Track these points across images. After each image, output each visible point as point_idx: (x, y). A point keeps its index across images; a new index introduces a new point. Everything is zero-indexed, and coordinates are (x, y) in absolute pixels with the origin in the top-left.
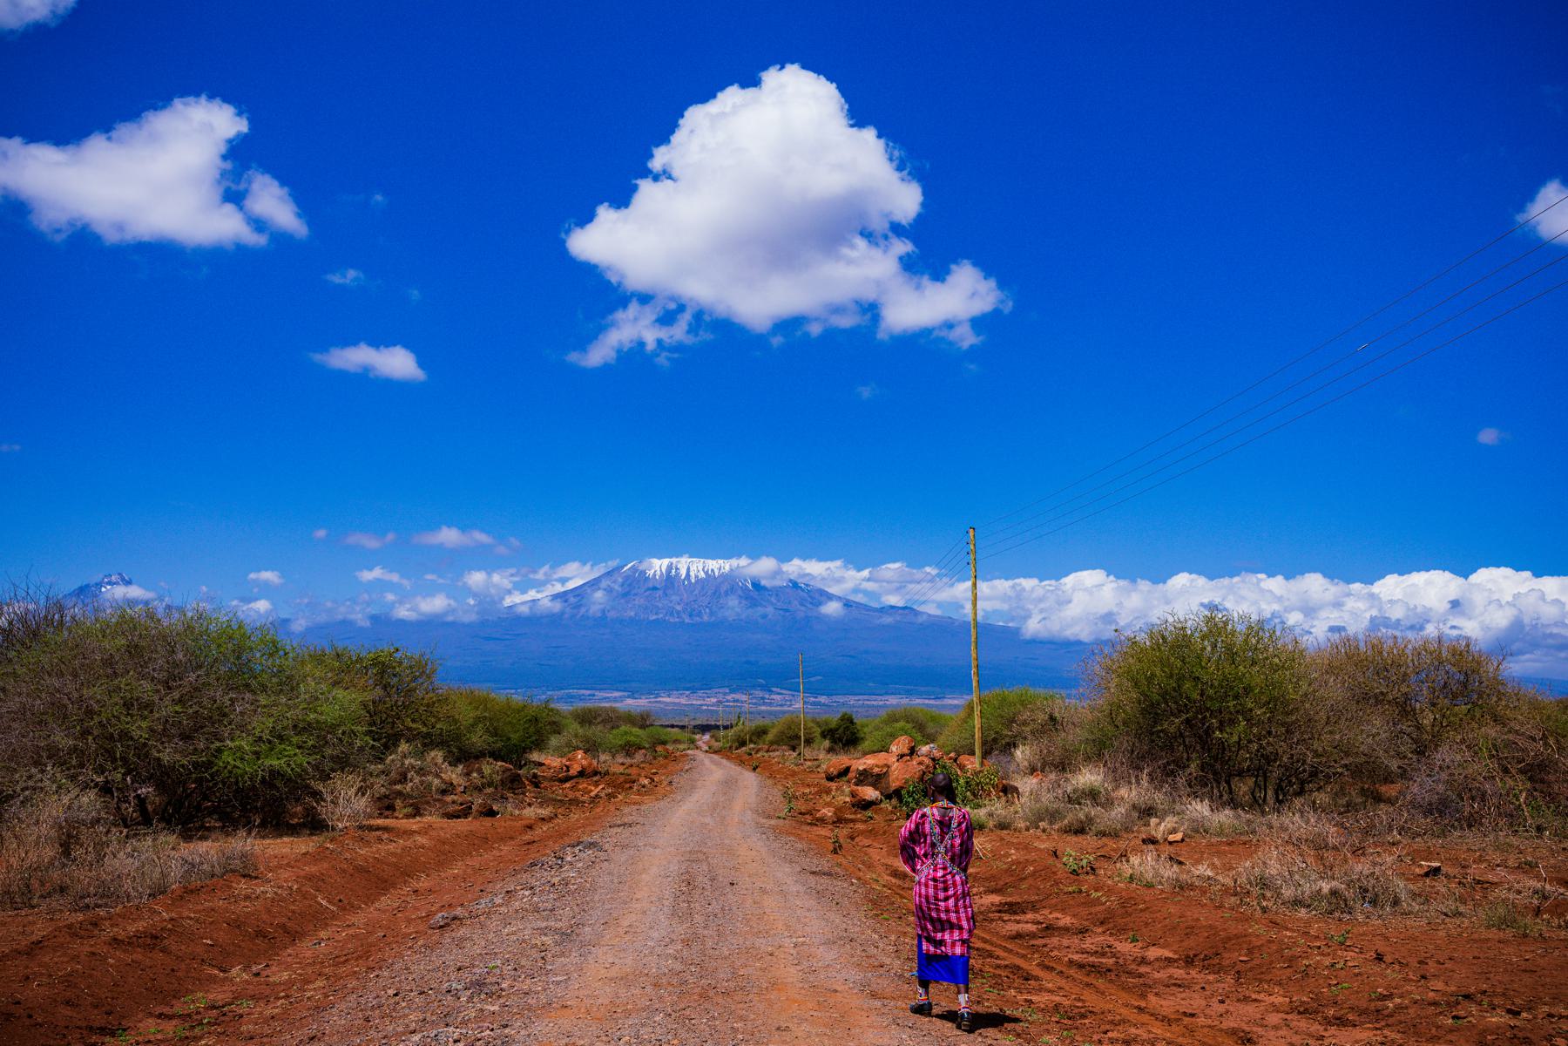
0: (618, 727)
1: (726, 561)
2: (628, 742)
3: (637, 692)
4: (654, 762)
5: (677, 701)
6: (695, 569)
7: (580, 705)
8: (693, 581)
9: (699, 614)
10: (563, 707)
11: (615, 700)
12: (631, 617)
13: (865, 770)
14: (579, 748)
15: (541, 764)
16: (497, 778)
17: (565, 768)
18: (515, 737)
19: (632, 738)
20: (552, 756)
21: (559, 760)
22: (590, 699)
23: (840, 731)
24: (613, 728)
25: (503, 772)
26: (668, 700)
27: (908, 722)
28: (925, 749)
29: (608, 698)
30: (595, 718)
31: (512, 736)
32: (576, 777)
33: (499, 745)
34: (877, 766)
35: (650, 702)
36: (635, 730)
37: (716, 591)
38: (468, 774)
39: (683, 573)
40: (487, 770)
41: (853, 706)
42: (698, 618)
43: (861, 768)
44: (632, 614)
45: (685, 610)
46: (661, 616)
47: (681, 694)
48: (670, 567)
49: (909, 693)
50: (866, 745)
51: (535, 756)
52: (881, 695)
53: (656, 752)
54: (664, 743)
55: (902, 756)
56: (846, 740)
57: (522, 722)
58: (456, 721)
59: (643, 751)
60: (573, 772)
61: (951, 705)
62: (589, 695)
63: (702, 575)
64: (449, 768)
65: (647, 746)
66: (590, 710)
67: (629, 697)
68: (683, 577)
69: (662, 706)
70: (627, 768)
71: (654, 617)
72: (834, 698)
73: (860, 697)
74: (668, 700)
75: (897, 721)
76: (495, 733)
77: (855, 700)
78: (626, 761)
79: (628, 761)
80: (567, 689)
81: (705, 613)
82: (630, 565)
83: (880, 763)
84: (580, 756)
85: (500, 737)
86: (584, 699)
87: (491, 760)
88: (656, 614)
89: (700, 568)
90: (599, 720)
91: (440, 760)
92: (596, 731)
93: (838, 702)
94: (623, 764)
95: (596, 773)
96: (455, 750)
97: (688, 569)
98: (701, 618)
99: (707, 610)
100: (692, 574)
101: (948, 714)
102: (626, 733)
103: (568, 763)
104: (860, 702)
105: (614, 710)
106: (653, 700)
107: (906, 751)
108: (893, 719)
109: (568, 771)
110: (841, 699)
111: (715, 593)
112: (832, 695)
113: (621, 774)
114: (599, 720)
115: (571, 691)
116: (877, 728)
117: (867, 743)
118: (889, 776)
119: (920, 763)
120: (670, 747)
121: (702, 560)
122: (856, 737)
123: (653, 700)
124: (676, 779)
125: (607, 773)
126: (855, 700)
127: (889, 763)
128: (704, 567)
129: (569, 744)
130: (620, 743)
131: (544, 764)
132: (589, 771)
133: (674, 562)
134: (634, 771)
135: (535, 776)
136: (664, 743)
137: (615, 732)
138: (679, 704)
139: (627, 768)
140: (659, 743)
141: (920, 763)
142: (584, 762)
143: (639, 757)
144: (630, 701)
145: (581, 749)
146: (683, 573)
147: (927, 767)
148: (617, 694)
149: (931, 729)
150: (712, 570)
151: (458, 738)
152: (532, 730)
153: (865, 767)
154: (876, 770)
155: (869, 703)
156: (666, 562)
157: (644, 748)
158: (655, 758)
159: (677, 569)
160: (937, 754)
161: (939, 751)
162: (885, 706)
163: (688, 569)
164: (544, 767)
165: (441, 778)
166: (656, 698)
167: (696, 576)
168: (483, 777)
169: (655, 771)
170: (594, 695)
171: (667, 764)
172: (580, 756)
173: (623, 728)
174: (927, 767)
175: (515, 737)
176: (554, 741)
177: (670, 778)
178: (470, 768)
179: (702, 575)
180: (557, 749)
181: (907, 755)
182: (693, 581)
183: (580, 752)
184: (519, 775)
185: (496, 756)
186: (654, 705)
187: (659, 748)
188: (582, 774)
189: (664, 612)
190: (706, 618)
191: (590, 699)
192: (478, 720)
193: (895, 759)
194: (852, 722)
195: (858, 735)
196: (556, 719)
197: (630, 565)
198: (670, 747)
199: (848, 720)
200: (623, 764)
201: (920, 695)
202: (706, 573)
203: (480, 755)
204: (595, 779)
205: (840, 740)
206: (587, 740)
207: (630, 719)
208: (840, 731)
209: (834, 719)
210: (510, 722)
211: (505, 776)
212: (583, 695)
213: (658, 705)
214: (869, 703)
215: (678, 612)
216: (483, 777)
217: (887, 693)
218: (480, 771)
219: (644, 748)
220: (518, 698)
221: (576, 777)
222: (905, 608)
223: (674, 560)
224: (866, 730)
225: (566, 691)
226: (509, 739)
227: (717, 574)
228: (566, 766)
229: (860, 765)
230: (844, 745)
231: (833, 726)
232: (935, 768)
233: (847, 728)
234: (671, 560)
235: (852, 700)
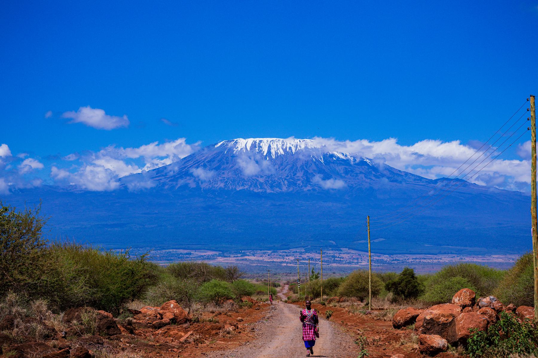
0: (209, 280)
1: (301, 140)
2: (218, 293)
3: (227, 251)
4: (240, 310)
5: (261, 259)
6: (275, 147)
7: (176, 262)
8: (274, 157)
9: (279, 186)
10: (162, 264)
11: (209, 258)
12: (220, 188)
13: (431, 319)
14: (172, 298)
15: (137, 312)
16: (94, 325)
17: (159, 316)
18: (113, 288)
19: (221, 290)
20: (149, 305)
21: (153, 309)
22: (187, 257)
23: (403, 284)
24: (205, 281)
25: (100, 319)
26: (252, 258)
27: (463, 277)
28: (485, 300)
29: (202, 256)
30: (189, 273)
31: (111, 287)
32: (169, 324)
33: (99, 295)
34: (443, 316)
35: (238, 260)
36: (223, 283)
37: (293, 165)
38: (68, 321)
39: (265, 150)
40: (85, 317)
41: (412, 264)
42: (278, 189)
43: (428, 317)
44: (222, 185)
45: (266, 182)
46: (246, 187)
47: (264, 253)
48: (254, 145)
49: (459, 253)
50: (427, 296)
51: (134, 305)
52: (436, 254)
53: (242, 301)
54: (249, 294)
55: (464, 307)
56: (408, 292)
57: (119, 275)
58: (58, 274)
59: (231, 301)
60: (166, 320)
61: (496, 263)
62: (187, 254)
63: (281, 152)
64: (52, 315)
65: (234, 297)
66: (185, 266)
67: (219, 256)
68: (265, 154)
69: (248, 263)
70: (216, 316)
71: (241, 188)
72: (395, 257)
73: (418, 256)
74: (252, 258)
75: (454, 276)
76: (96, 285)
77: (413, 259)
78: (215, 309)
79: (217, 309)
80: (168, 249)
81: (284, 184)
82: (219, 144)
83: (447, 313)
84: (172, 305)
85: (100, 288)
86: (181, 257)
87: (89, 309)
88: (243, 185)
89: (280, 146)
90: (193, 273)
91: (45, 308)
92: (189, 284)
93: (398, 260)
94: (213, 312)
95: (187, 320)
96: (57, 299)
97: (270, 146)
98: (282, 190)
99: (286, 182)
100: (273, 151)
101: (498, 269)
102: (215, 285)
103: (161, 312)
104: (418, 260)
105: (206, 266)
106: (240, 258)
107: (468, 302)
108: (450, 273)
109: (162, 318)
110: (401, 258)
111: (292, 168)
112: (392, 254)
113: (210, 321)
114: (193, 273)
115: (171, 250)
116: (436, 282)
117: (427, 295)
118: (455, 325)
119: (484, 313)
120: (254, 298)
121: (281, 139)
122: (417, 290)
123: (240, 258)
124: (258, 326)
125: (197, 321)
126: (413, 259)
127: (454, 313)
128: (283, 145)
129: (163, 295)
130: (211, 293)
131: (140, 312)
132: (181, 318)
133: (258, 142)
134: (222, 318)
135: (130, 323)
136: (249, 294)
137: (206, 284)
138: (262, 261)
139: (216, 316)
140: (245, 295)
141: (484, 313)
142: (176, 311)
143: (227, 306)
144: (220, 259)
145: (174, 299)
146: (265, 150)
147: (490, 316)
148: (210, 253)
149: (484, 282)
150: (290, 148)
151: (61, 289)
152: (128, 282)
153: (432, 316)
154: (442, 319)
155: (425, 261)
156: (250, 141)
157: (231, 298)
158: (241, 307)
159: (260, 147)
160: (497, 305)
161: (498, 303)
162: (439, 264)
163: (270, 146)
164: (140, 315)
165: (44, 324)
166: (242, 256)
167: (276, 153)
168: (81, 324)
169: (239, 318)
170: (190, 254)
171: (252, 312)
172: (172, 305)
173: (213, 281)
174: (490, 316)
175: (113, 288)
176: (151, 292)
177: (252, 325)
178: (71, 316)
179: (281, 152)
180: (154, 299)
181: (469, 306)
182: (274, 157)
183: (172, 301)
184: (115, 322)
185: (95, 304)
186: (241, 262)
187: (245, 299)
188: (174, 321)
189: (250, 184)
190: (284, 189)
191: (187, 257)
192: (80, 273)
193: (459, 309)
194: (413, 276)
195: (418, 288)
196: (155, 273)
197: (219, 144)
198: (254, 298)
199: (409, 275)
200: (213, 312)
201: (470, 254)
202: (285, 150)
203: (80, 305)
204: (185, 325)
205: (403, 292)
206: (179, 291)
207: (219, 273)
208: (403, 284)
209: (397, 273)
210: (109, 275)
211: (102, 323)
212: (181, 254)
213: (244, 262)
214: (425, 261)
215: (261, 184)
216: (81, 324)
217: (440, 253)
218: (79, 318)
219: (231, 298)
220: (117, 254)
221: (169, 324)
222: (457, 180)
223: (258, 140)
224: (425, 283)
225: (168, 251)
226: (108, 290)
227: (294, 150)
228: (159, 314)
229: (427, 314)
230: (406, 297)
231: (396, 280)
232: (498, 318)
233: (409, 282)
234: (255, 139)
235: (410, 258)
